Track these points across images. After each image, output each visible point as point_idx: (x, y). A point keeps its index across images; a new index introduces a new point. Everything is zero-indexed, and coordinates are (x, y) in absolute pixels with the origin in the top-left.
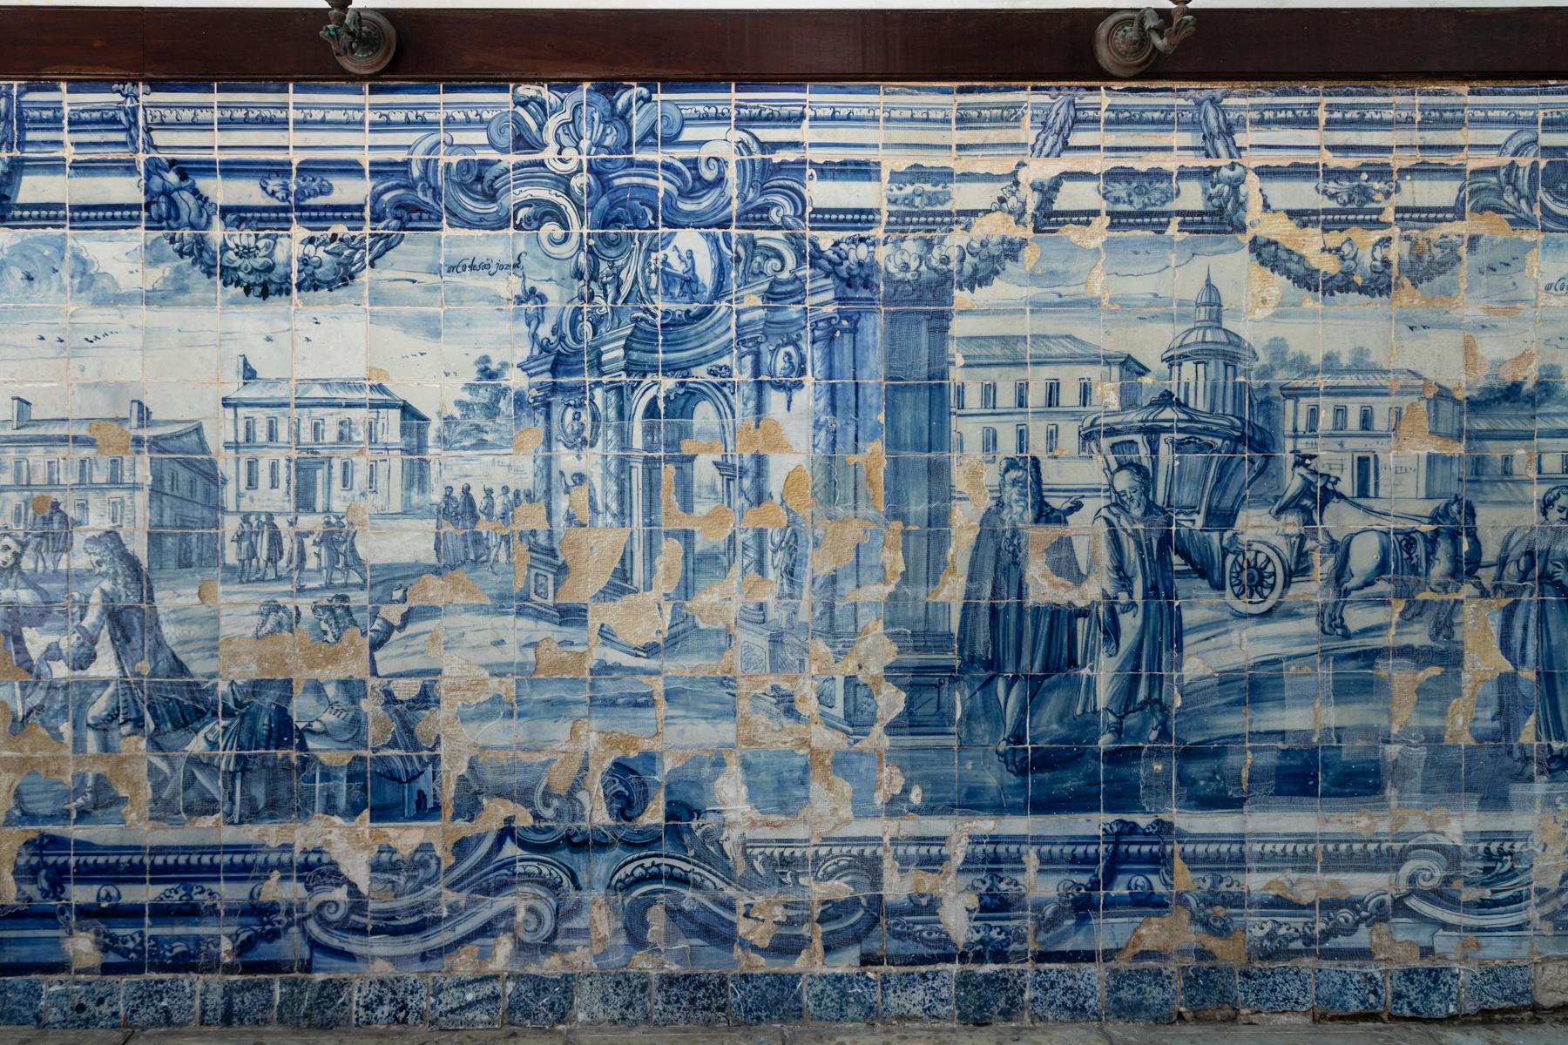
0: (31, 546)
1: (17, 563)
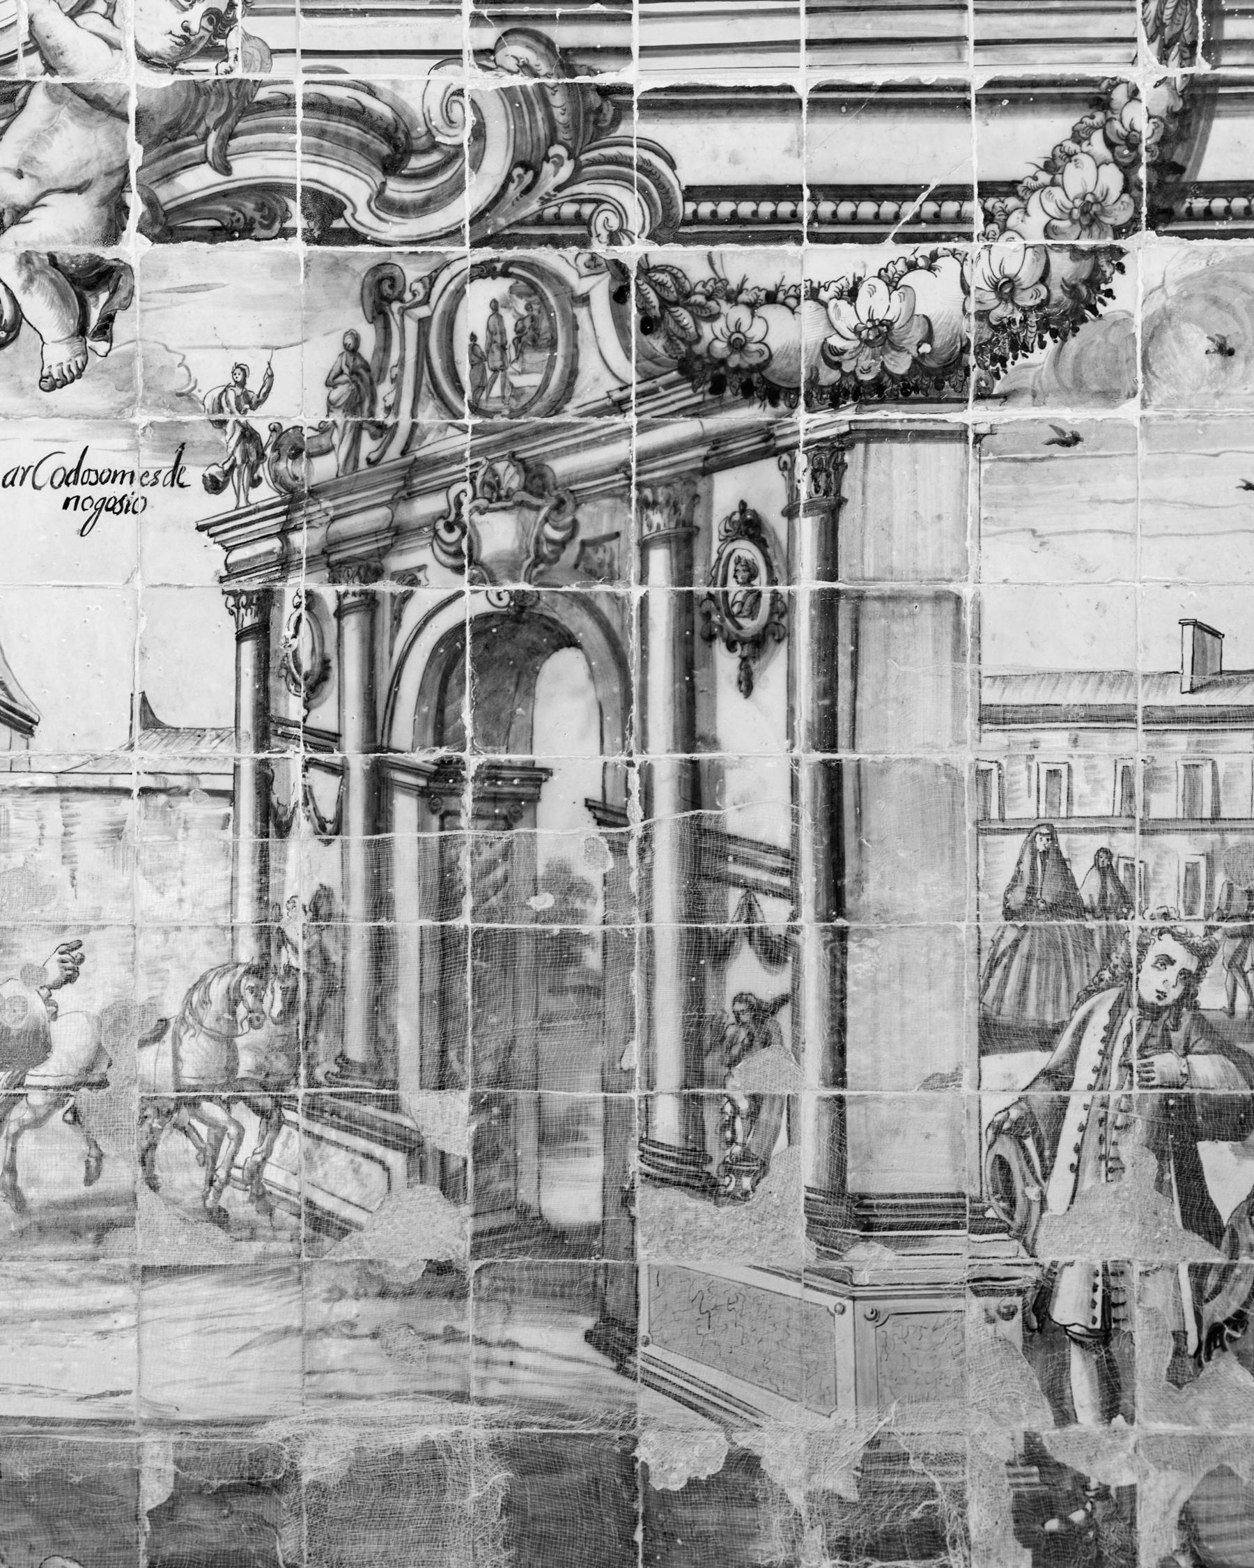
0: (1218, 960)
1: (1188, 998)
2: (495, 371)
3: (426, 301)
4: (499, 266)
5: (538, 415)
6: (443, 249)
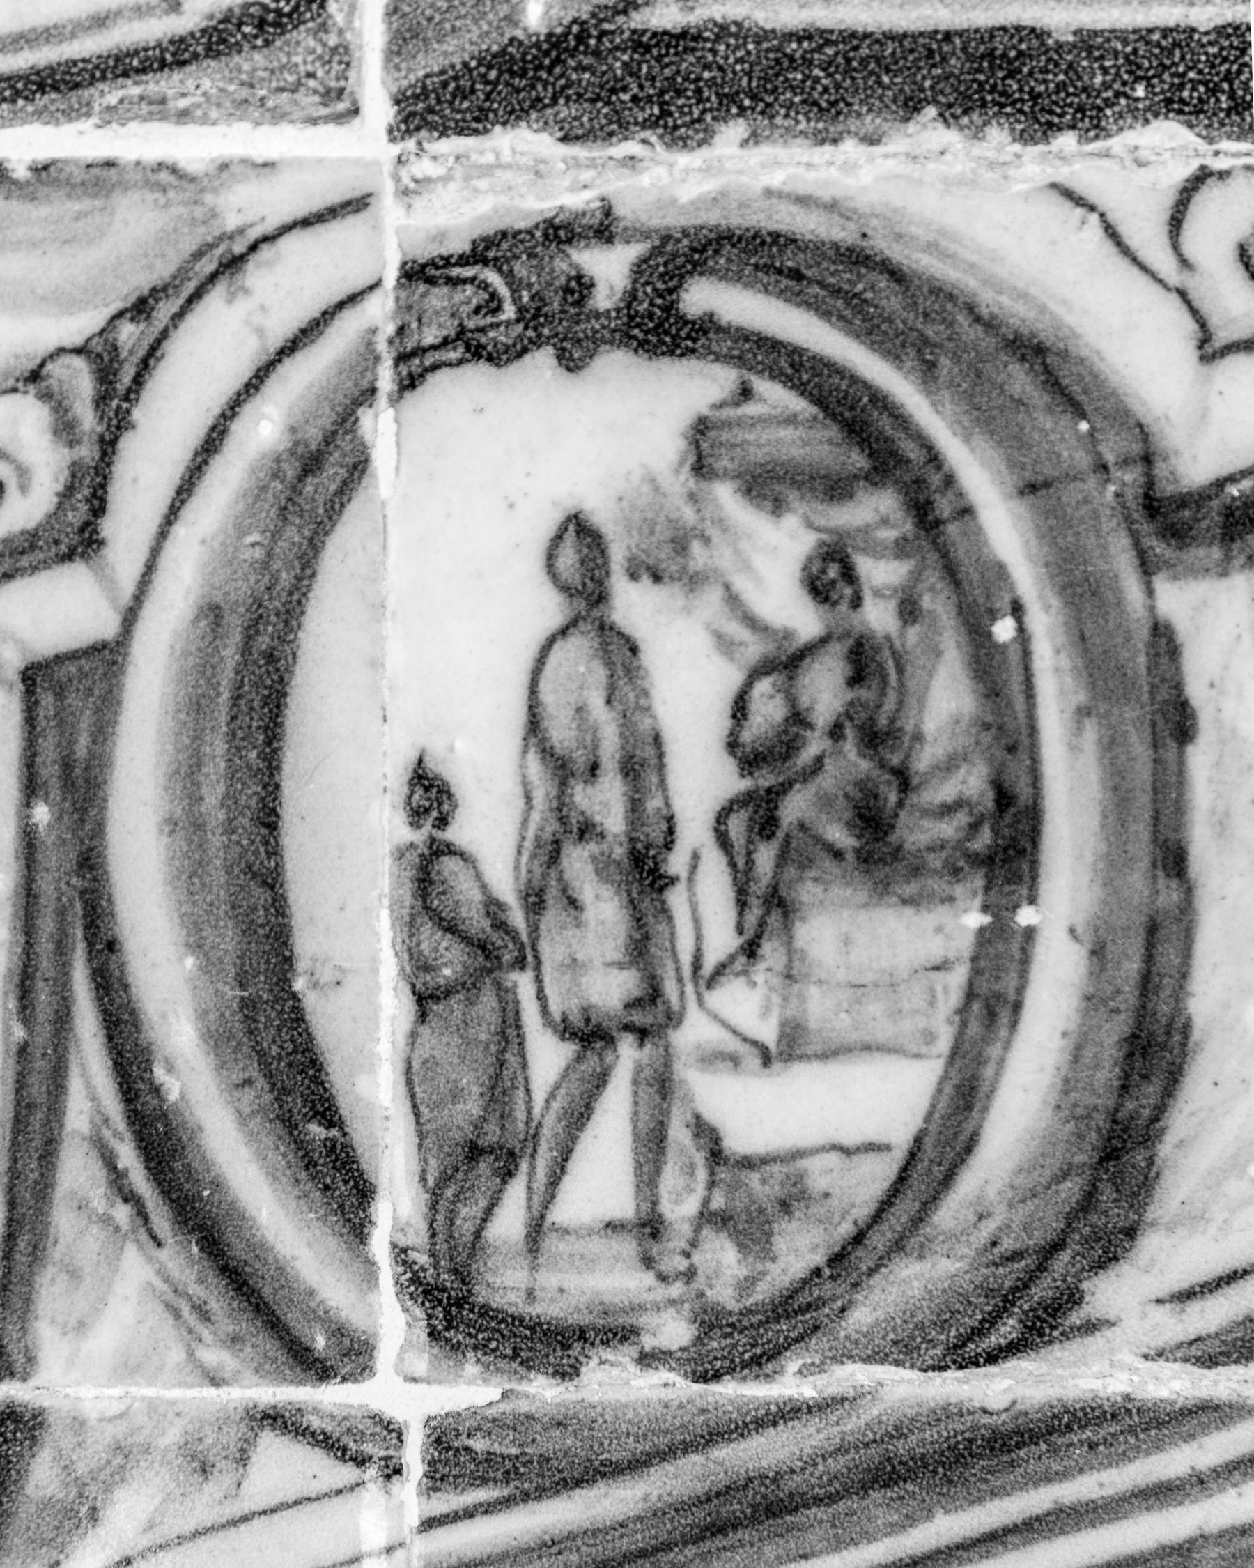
2: (589, 1035)
3: (76, 533)
4: (609, 269)
5: (902, 1348)
6: (194, 147)
